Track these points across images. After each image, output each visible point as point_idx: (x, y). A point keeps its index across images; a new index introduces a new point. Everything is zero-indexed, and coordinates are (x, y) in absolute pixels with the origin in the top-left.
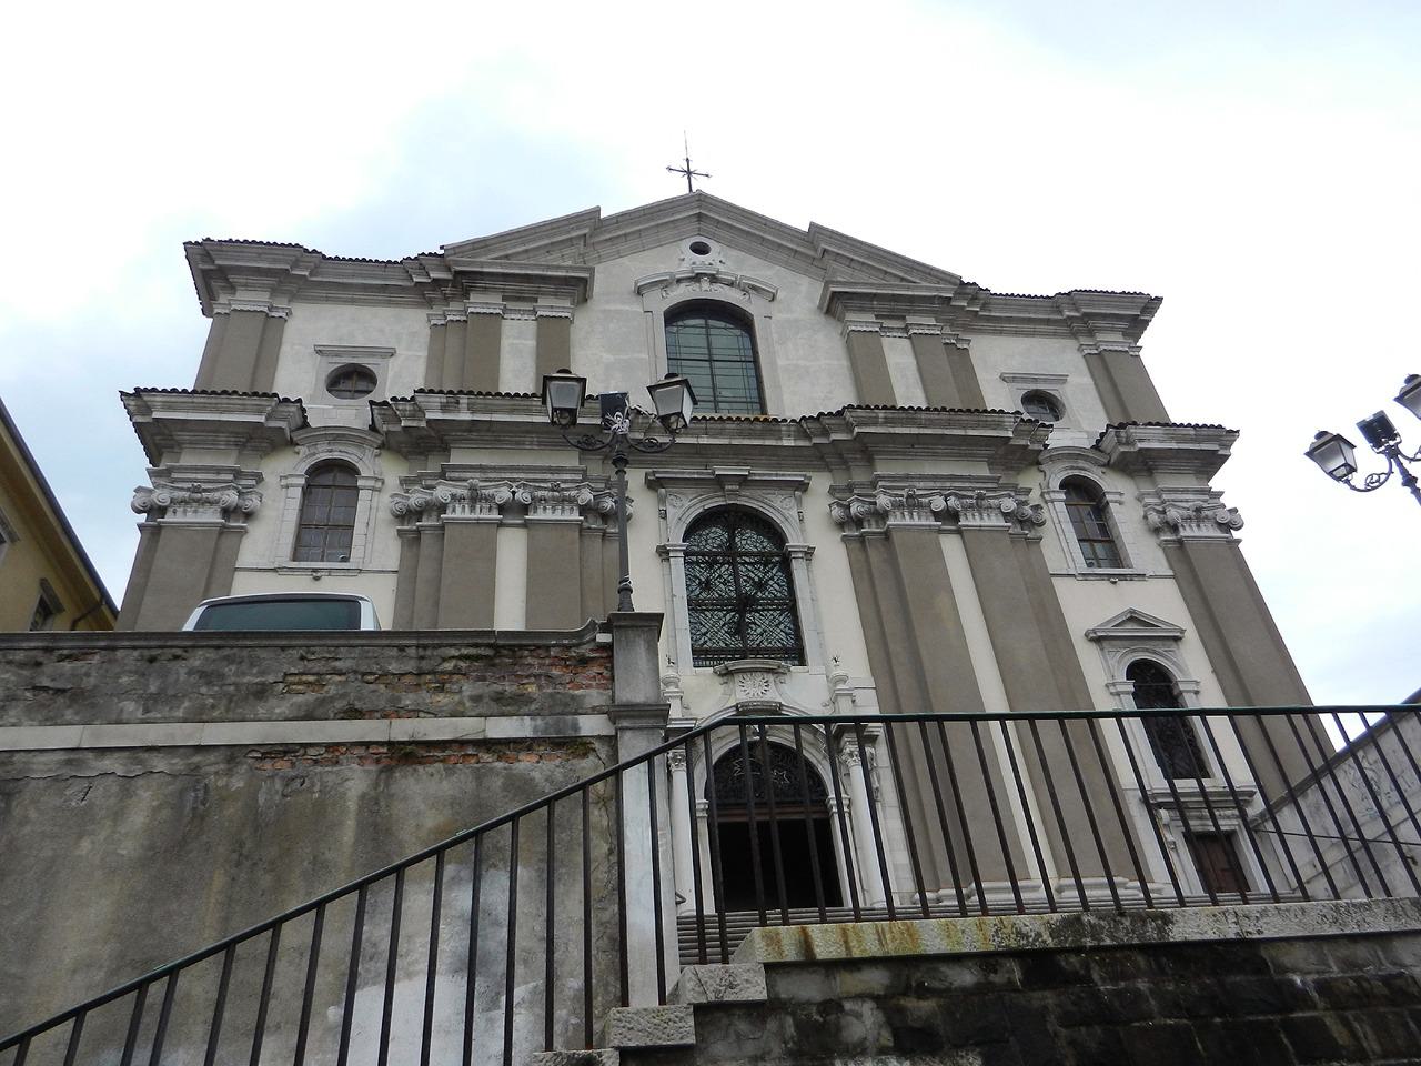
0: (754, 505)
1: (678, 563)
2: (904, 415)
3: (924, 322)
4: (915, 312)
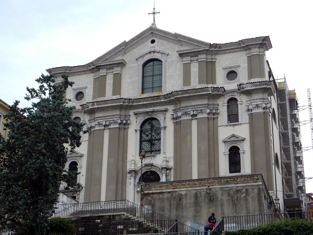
0: (155, 117)
1: (138, 133)
2: (185, 92)
3: (202, 57)
4: (200, 54)
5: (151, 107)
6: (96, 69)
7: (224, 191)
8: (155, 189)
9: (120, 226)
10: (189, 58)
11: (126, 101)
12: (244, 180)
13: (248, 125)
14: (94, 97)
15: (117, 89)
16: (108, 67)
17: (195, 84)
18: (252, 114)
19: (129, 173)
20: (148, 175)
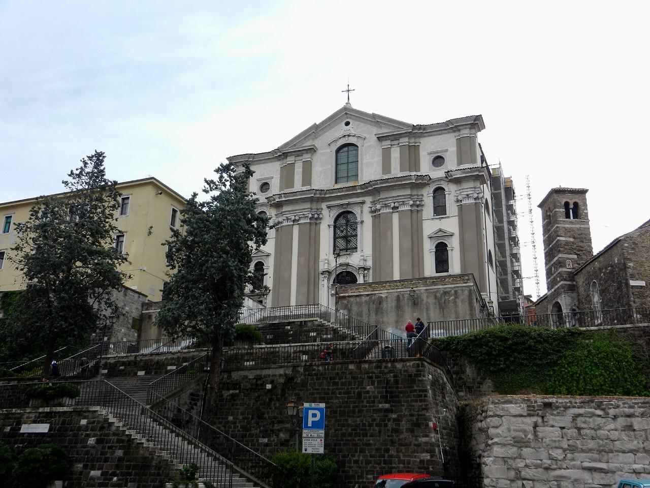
1: (332, 229)
3: (404, 141)
4: (402, 137)
5: (346, 199)
6: (283, 157)
7: (430, 293)
8: (351, 291)
9: (312, 333)
10: (389, 142)
11: (318, 192)
12: (453, 281)
13: (457, 218)
14: (281, 189)
15: (307, 179)
16: (295, 153)
17: (396, 171)
18: (461, 205)
19: (322, 274)
20: (343, 276)
